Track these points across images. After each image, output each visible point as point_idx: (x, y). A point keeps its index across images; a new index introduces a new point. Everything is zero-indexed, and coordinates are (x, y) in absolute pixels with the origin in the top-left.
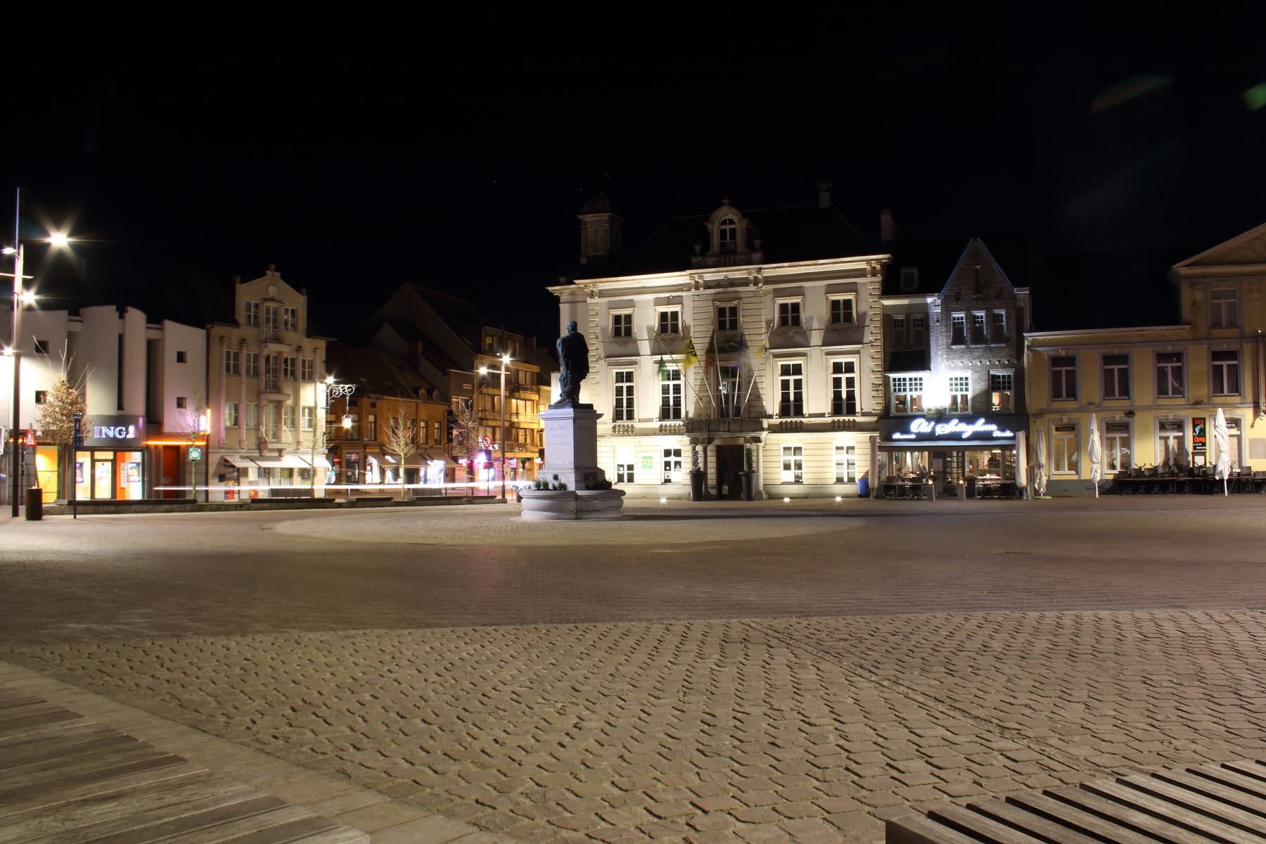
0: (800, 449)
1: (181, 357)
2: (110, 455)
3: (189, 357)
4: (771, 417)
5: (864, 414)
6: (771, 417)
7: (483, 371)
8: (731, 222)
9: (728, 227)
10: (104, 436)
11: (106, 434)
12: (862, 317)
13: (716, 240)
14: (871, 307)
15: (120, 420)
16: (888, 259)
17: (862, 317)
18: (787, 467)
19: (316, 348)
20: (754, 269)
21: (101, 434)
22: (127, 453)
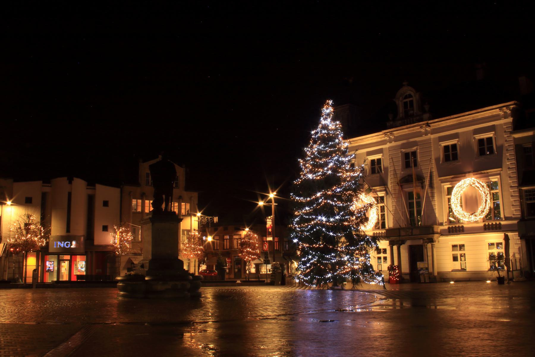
0: (463, 245)
1: (106, 204)
2: (68, 257)
3: (110, 204)
4: (441, 224)
5: (507, 219)
6: (441, 224)
7: (261, 203)
8: (410, 96)
9: (408, 100)
10: (58, 247)
11: (60, 246)
12: (500, 148)
13: (401, 109)
14: (506, 141)
15: (67, 238)
16: (514, 104)
17: (500, 148)
18: (455, 259)
19: (191, 197)
20: (424, 124)
21: (57, 246)
22: (47, 256)
